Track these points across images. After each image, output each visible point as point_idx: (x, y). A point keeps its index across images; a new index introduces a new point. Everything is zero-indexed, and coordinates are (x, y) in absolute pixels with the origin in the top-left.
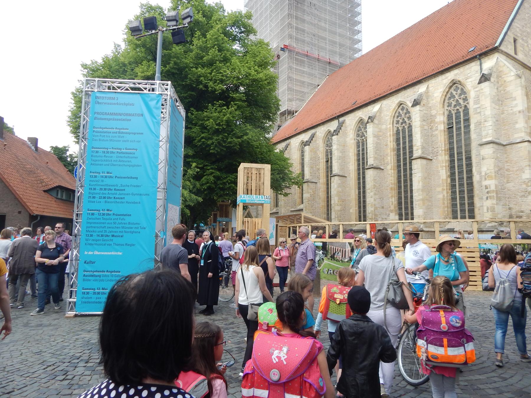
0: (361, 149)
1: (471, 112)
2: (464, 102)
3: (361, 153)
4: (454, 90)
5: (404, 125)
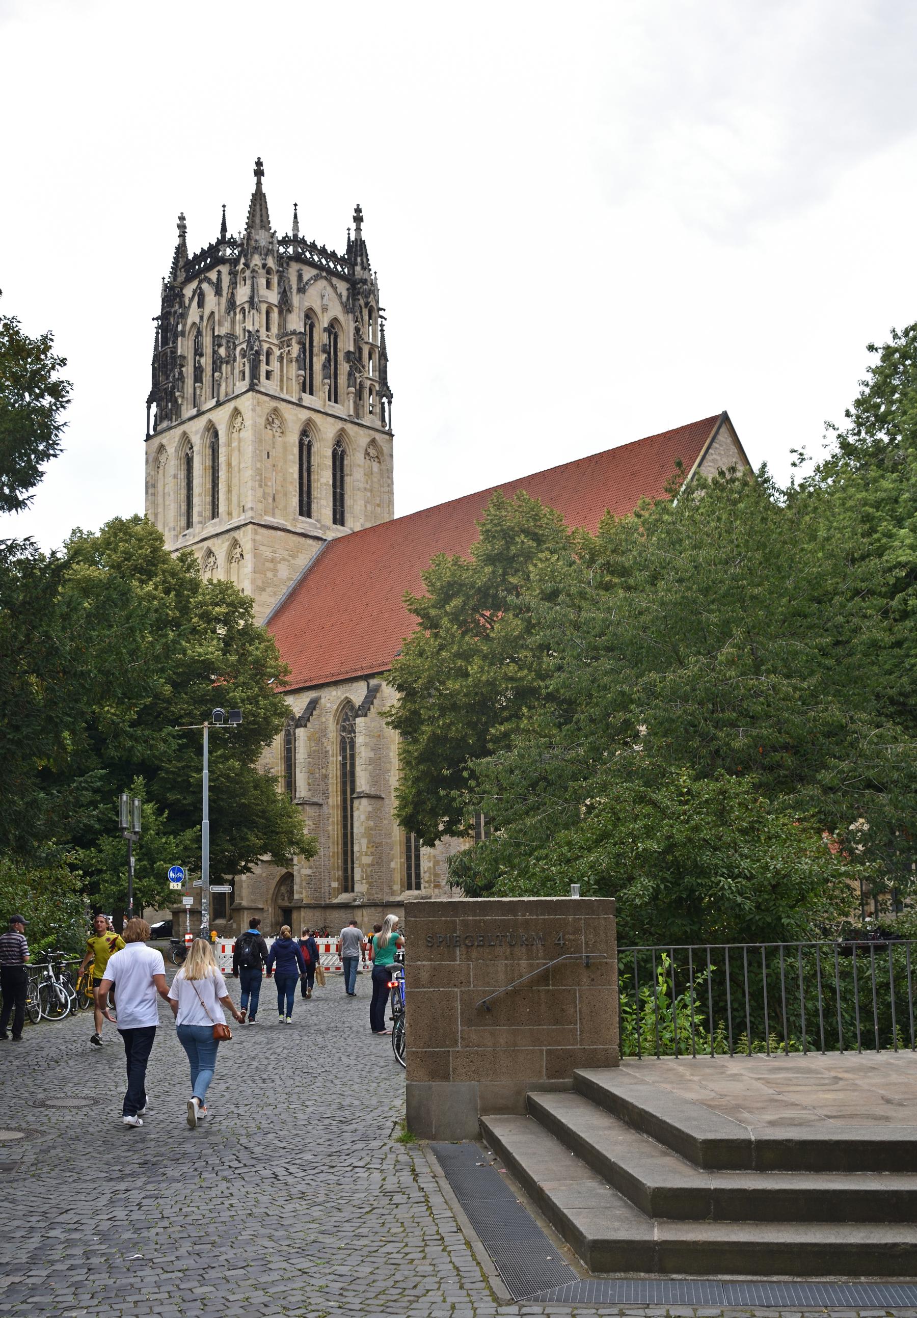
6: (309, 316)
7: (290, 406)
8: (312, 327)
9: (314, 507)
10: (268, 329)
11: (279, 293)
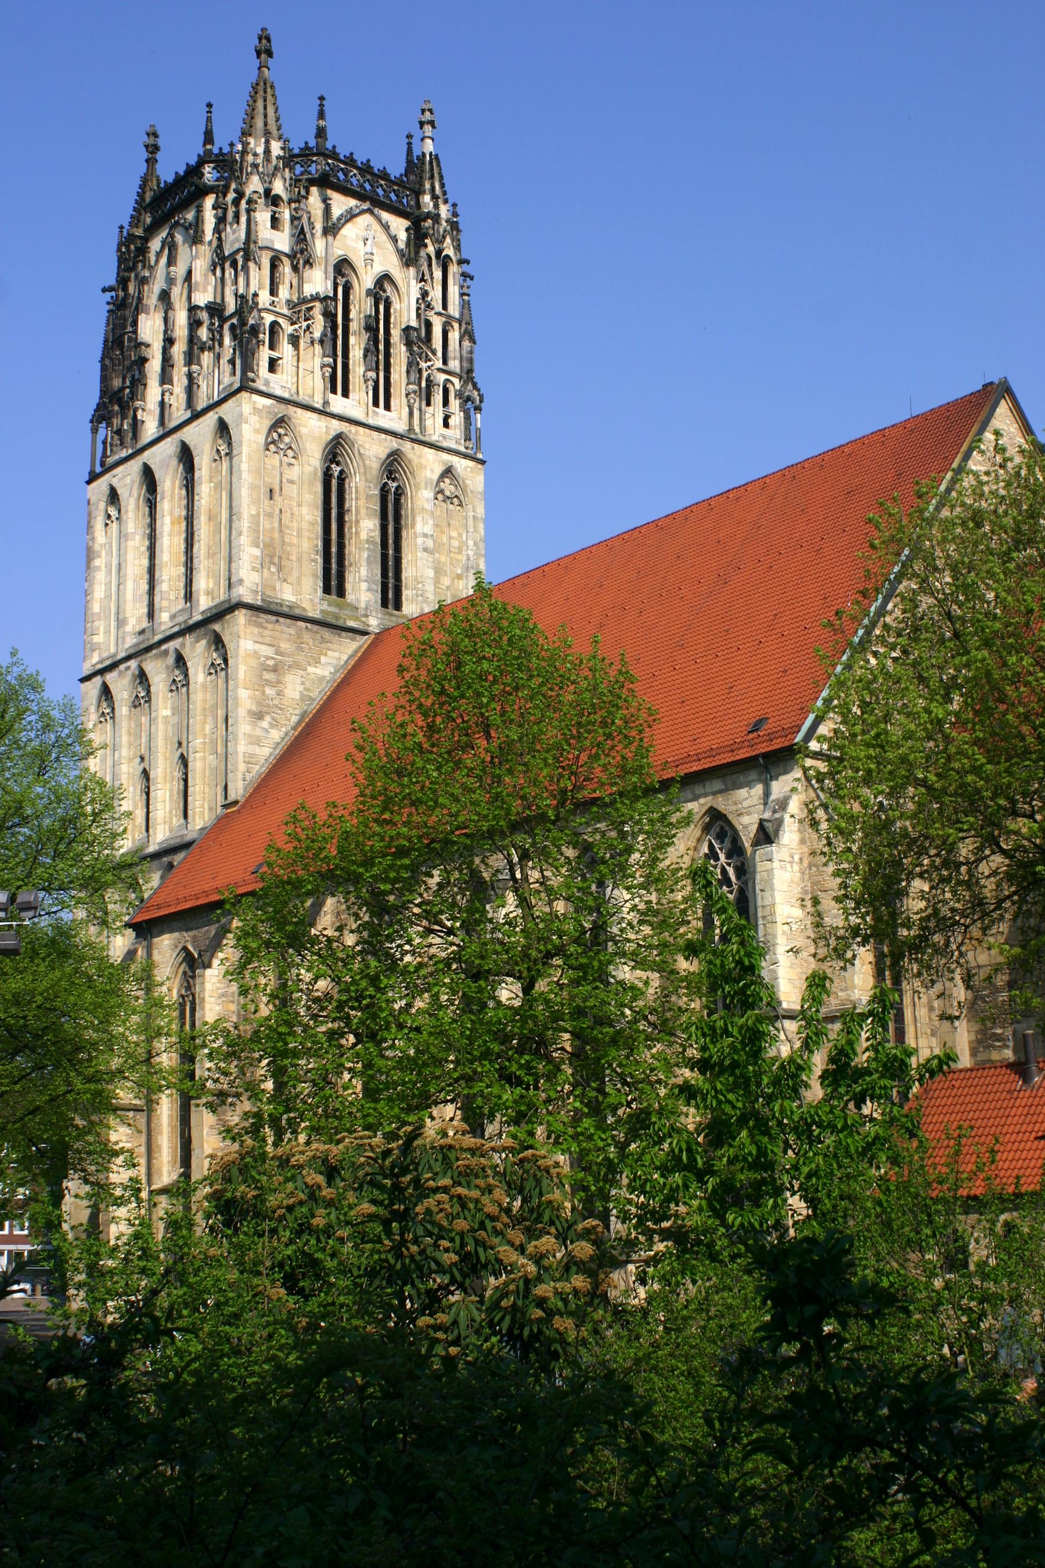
6: (342, 267)
8: (347, 289)
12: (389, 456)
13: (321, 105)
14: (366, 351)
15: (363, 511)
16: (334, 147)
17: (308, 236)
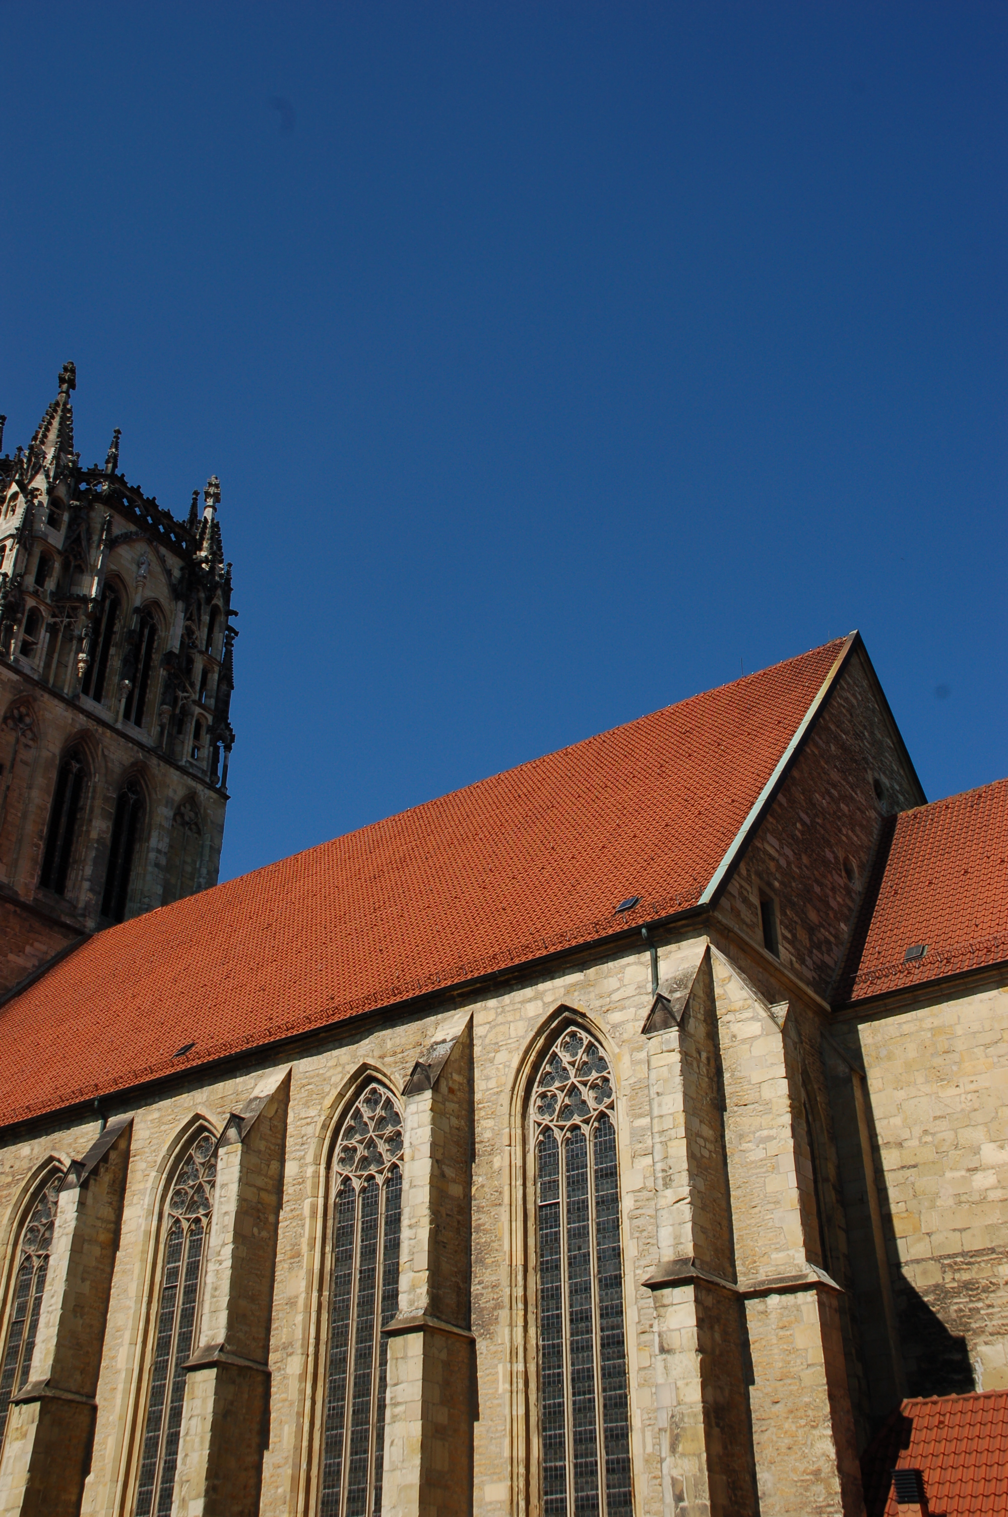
0: (183, 1265)
1: (623, 1140)
2: (599, 1100)
3: (181, 1283)
4: (565, 1046)
5: (373, 1169)
7: (56, 702)
8: (116, 604)
9: (72, 875)
10: (40, 581)
11: (67, 537)
12: (133, 764)
13: (117, 438)
14: (125, 661)
15: (97, 811)
16: (123, 475)
17: (84, 543)
